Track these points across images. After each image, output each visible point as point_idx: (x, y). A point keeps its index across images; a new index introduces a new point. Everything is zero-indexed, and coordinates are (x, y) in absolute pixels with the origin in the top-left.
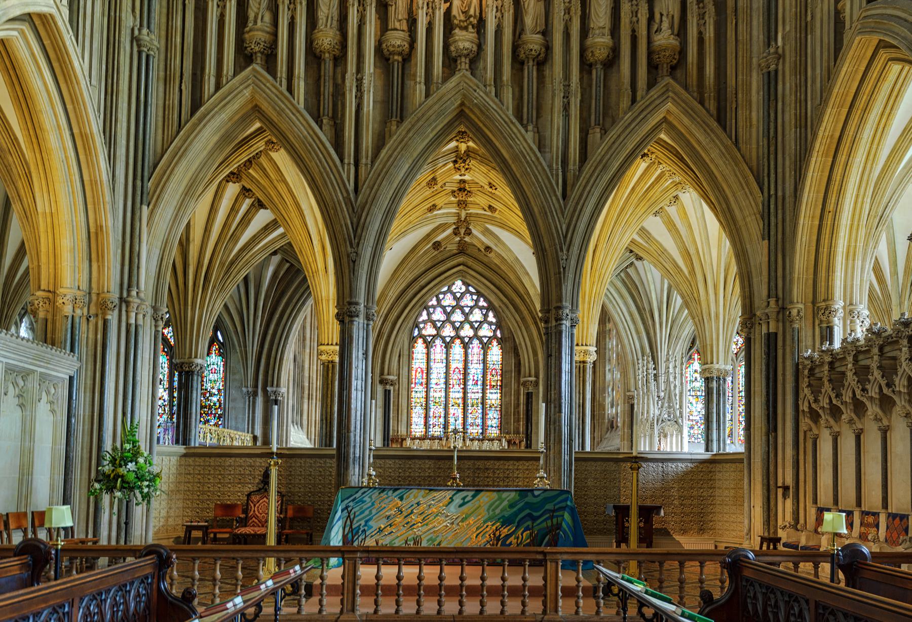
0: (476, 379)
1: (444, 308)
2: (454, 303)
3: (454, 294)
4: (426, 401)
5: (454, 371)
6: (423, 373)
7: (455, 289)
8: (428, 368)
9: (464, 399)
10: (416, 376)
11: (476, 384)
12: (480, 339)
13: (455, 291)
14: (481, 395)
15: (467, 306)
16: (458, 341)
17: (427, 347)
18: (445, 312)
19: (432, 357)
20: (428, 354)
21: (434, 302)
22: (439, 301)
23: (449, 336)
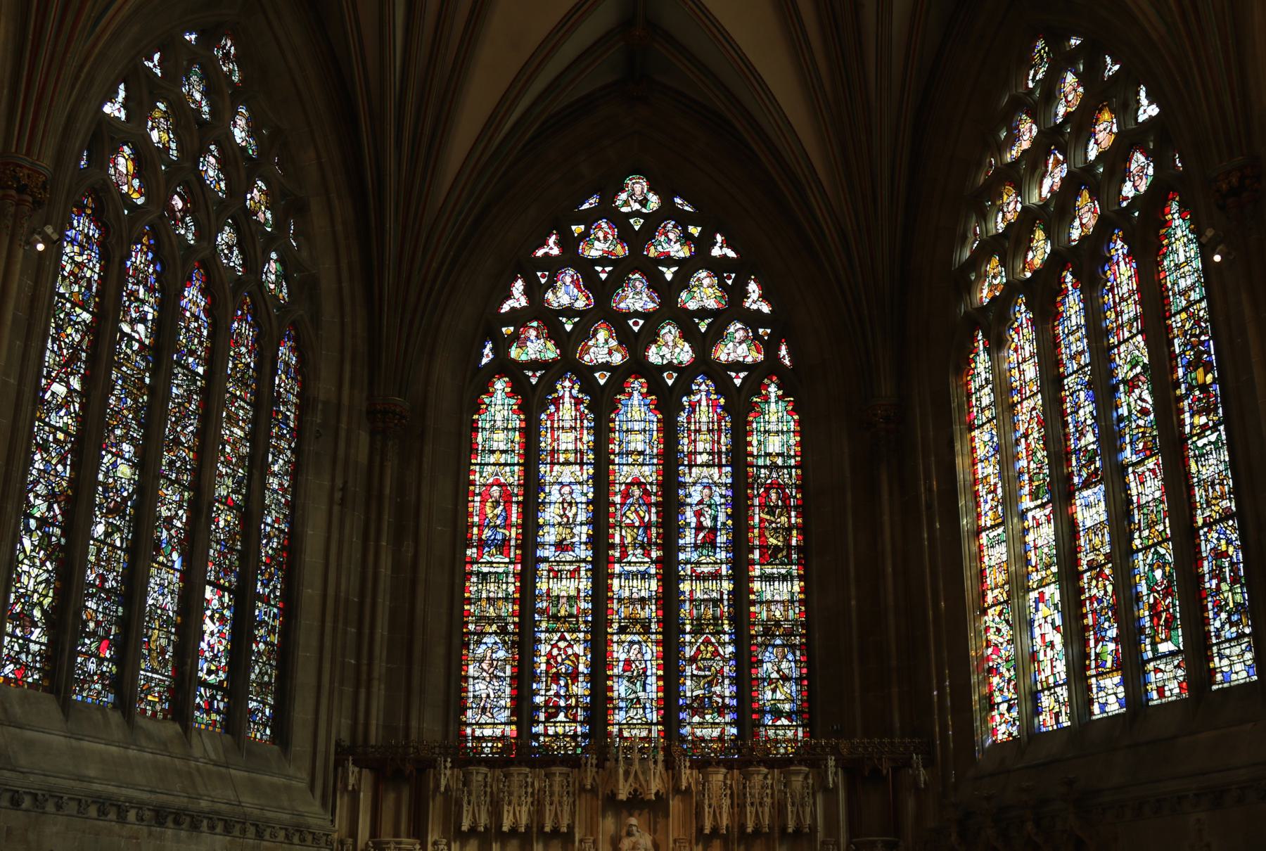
0: (707, 522)
1: (586, 268)
2: (621, 251)
3: (620, 221)
4: (521, 614)
5: (626, 495)
6: (508, 503)
7: (625, 202)
8: (532, 487)
9: (669, 599)
10: (483, 514)
11: (710, 543)
12: (718, 373)
13: (625, 210)
14: (727, 586)
15: (668, 260)
16: (637, 385)
17: (522, 409)
18: (589, 281)
19: (546, 442)
20: (530, 433)
21: (552, 248)
22: (568, 243)
23: (606, 366)
